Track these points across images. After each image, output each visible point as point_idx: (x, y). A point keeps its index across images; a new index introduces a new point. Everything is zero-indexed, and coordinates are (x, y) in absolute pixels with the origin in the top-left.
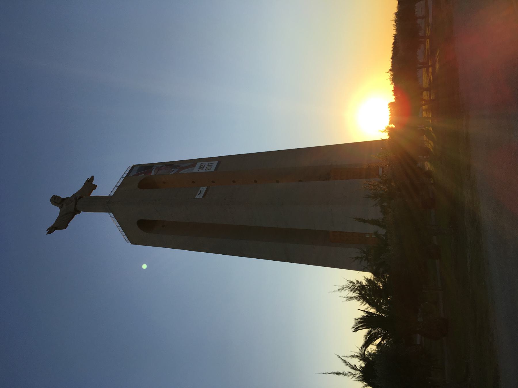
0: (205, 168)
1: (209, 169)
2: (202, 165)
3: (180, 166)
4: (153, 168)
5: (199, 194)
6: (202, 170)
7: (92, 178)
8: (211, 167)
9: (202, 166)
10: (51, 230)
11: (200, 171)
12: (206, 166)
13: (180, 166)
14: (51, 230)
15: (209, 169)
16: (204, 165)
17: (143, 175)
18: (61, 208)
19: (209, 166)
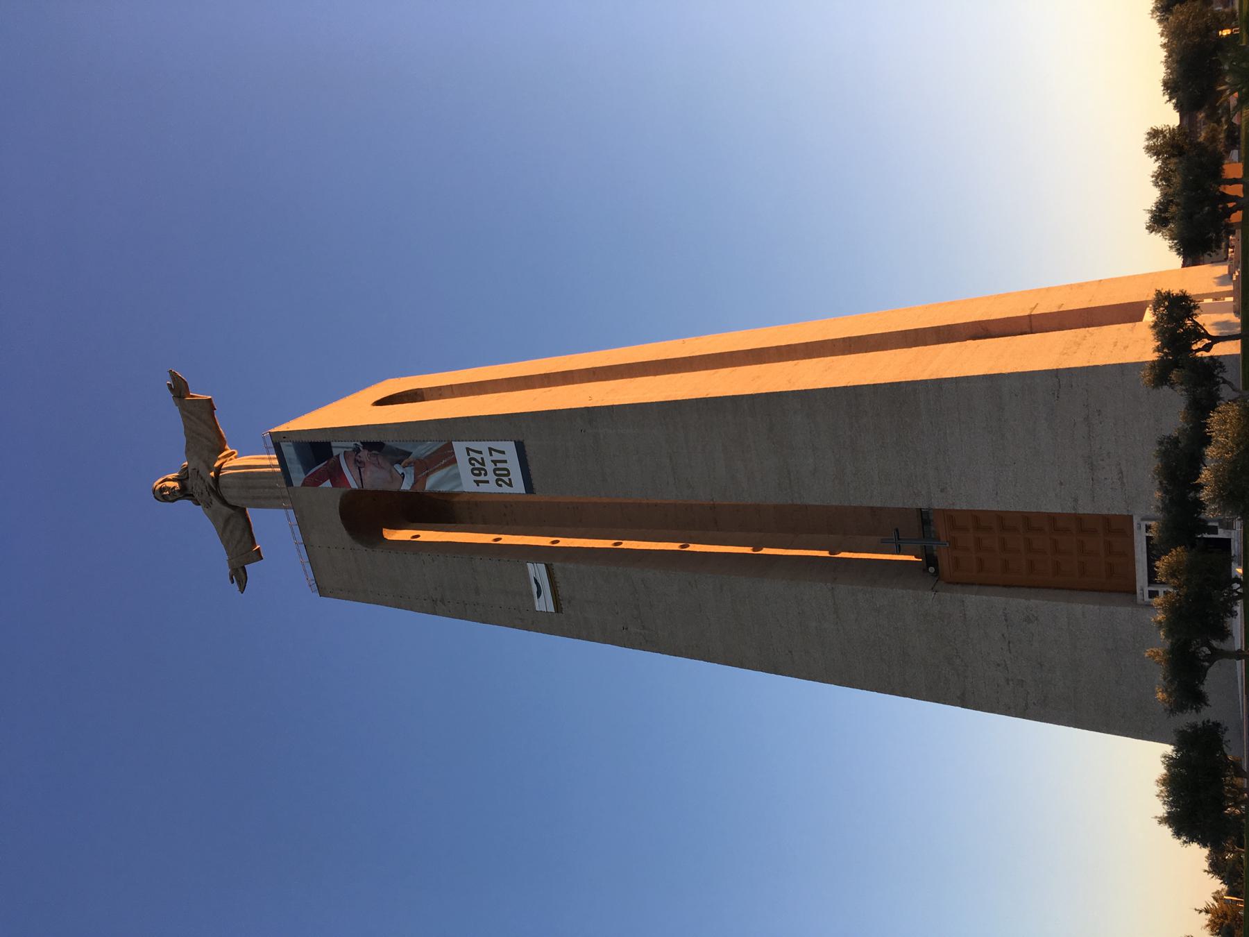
0: (491, 477)
1: (506, 479)
2: (473, 454)
3: (410, 454)
4: (335, 454)
5: (539, 595)
6: (487, 482)
7: (174, 376)
8: (505, 469)
9: (477, 465)
10: (239, 576)
11: (483, 488)
12: (489, 467)
13: (410, 454)
14: (239, 576)
15: (506, 479)
16: (478, 457)
17: (328, 484)
18: (199, 505)
19: (499, 465)
